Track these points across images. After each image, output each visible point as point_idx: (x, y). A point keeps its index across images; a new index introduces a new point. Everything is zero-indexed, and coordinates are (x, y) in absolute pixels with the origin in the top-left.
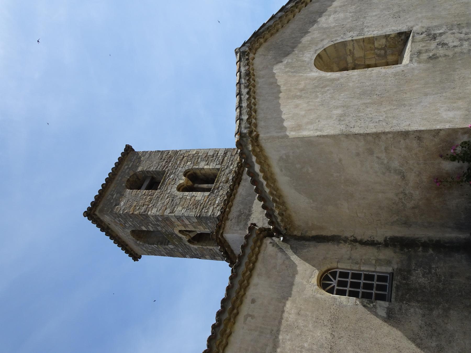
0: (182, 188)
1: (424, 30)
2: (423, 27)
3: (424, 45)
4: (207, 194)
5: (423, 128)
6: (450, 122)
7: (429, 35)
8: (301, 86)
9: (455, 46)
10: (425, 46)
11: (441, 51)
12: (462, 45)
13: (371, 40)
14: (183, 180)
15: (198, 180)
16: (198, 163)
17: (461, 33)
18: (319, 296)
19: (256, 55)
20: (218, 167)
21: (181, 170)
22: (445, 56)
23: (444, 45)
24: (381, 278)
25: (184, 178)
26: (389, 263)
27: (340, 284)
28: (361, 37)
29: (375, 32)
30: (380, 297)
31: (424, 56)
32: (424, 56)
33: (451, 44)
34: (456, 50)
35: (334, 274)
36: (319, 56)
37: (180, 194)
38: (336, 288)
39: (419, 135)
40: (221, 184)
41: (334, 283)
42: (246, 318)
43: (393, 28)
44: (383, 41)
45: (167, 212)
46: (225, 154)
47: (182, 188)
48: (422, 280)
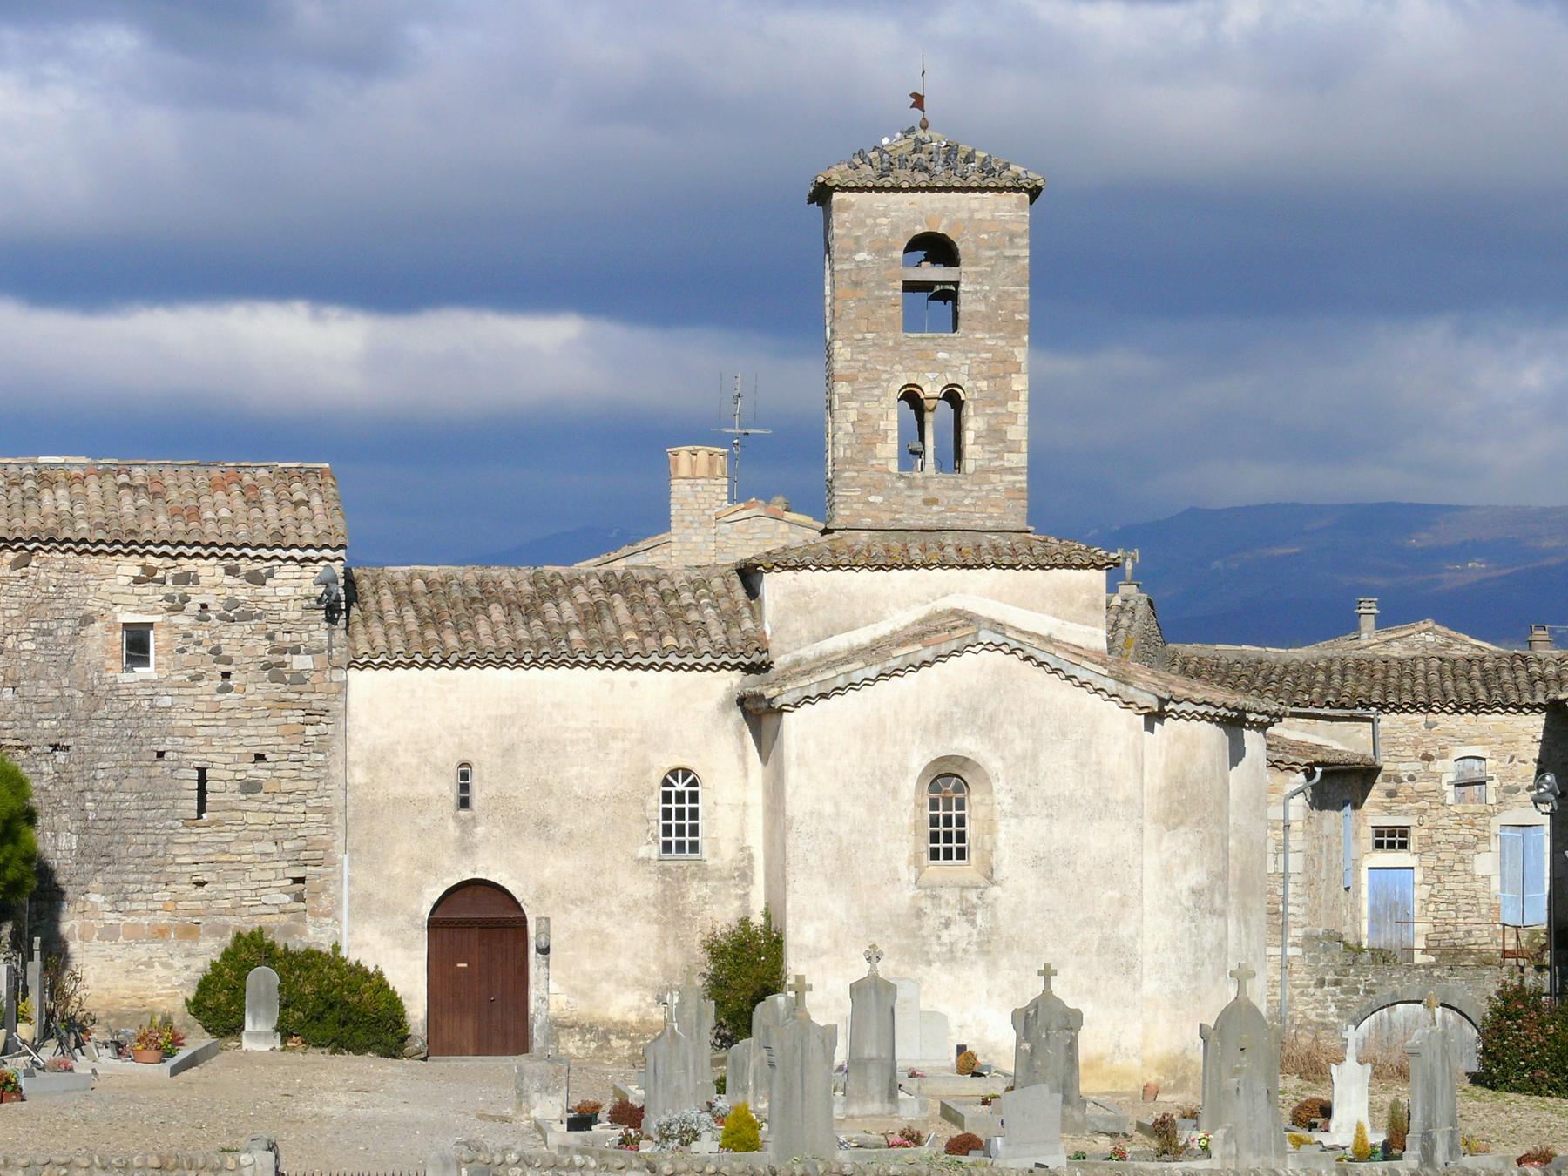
3: (952, 901)
4: (893, 466)
7: (974, 907)
18: (654, 773)
22: (921, 928)
23: (947, 925)
27: (680, 797)
30: (667, 847)
31: (926, 904)
32: (926, 904)
34: (934, 940)
35: (694, 783)
36: (966, 759)
38: (673, 790)
41: (680, 787)
43: (1006, 861)
44: (988, 847)
48: (692, 896)
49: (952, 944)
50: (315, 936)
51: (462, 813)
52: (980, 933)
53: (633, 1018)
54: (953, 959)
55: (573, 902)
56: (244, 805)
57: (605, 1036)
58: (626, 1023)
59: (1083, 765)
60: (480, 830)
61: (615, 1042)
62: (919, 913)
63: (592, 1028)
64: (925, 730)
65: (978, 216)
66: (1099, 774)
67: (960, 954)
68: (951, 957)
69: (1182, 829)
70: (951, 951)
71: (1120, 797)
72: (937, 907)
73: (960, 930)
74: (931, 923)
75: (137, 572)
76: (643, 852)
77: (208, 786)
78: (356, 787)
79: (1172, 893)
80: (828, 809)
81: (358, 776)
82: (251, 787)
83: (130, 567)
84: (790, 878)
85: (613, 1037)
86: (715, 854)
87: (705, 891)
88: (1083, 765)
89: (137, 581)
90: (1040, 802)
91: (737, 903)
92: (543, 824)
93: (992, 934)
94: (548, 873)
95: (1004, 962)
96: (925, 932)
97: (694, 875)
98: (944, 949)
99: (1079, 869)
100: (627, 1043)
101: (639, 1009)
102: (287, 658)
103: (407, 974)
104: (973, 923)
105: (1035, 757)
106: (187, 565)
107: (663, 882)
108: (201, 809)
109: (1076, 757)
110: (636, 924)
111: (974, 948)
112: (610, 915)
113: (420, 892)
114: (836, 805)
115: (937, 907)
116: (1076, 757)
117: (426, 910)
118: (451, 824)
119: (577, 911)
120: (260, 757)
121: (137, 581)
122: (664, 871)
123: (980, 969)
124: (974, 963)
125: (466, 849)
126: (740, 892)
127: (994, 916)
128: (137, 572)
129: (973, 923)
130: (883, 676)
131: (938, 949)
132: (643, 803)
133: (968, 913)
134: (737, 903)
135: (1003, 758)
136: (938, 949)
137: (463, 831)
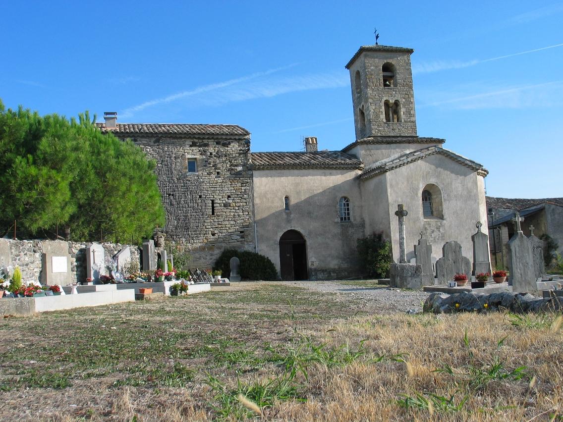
0: (387, 104)
2: (445, 224)
3: (434, 225)
4: (385, 121)
5: (391, 228)
6: (394, 236)
8: (414, 182)
12: (432, 238)
13: (441, 205)
14: (392, 101)
15: (392, 109)
16: (404, 106)
19: (436, 155)
20: (403, 121)
21: (398, 97)
23: (433, 232)
24: (349, 218)
25: (394, 101)
26: (355, 220)
28: (443, 201)
33: (433, 235)
34: (429, 236)
35: (347, 201)
36: (434, 185)
37: (382, 104)
39: (390, 228)
40: (391, 127)
42: (323, 173)
45: (370, 100)
47: (387, 104)
49: (434, 237)
50: (248, 248)
51: (287, 211)
53: (336, 267)
54: (435, 242)
55: (319, 235)
56: (225, 210)
57: (329, 273)
58: (335, 269)
59: (463, 186)
60: (292, 215)
61: (332, 274)
63: (326, 270)
70: (434, 239)
72: (430, 227)
73: (436, 234)
75: (191, 144)
76: (336, 220)
77: (215, 205)
78: (257, 204)
81: (257, 201)
82: (226, 205)
83: (189, 142)
84: (391, 220)
85: (332, 273)
86: (355, 220)
87: (353, 231)
88: (463, 186)
91: (361, 234)
92: (309, 213)
94: (311, 227)
96: (428, 234)
97: (350, 226)
98: (433, 239)
100: (335, 274)
101: (338, 264)
102: (236, 168)
103: (274, 257)
105: (451, 184)
106: (206, 141)
107: (342, 228)
108: (213, 213)
109: (461, 183)
110: (336, 241)
111: (440, 238)
112: (329, 238)
113: (277, 234)
114: (402, 198)
115: (430, 227)
116: (461, 183)
117: (279, 239)
118: (284, 214)
119: (320, 238)
120: (229, 197)
121: (191, 146)
122: (342, 226)
125: (289, 221)
126: (362, 230)
127: (445, 229)
128: (191, 144)
129: (440, 231)
130: (412, 161)
132: (335, 207)
133: (438, 228)
134: (361, 234)
135: (443, 184)
137: (288, 216)
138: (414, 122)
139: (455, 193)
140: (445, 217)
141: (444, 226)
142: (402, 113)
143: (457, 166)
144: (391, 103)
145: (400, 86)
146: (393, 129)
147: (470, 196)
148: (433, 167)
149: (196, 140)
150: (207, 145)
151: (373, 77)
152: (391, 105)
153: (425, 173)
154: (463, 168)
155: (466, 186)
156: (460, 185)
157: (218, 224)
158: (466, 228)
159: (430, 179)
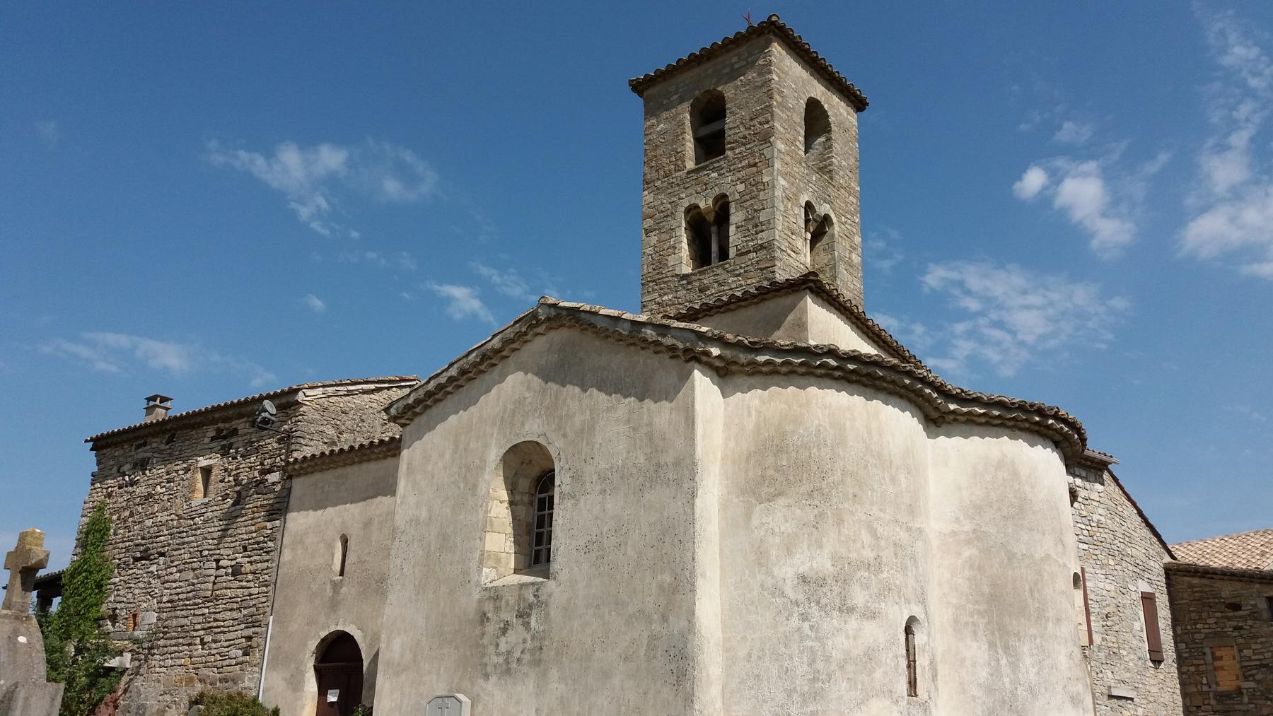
1: (542, 598)
2: (550, 596)
3: (511, 603)
6: (388, 647)
7: (530, 606)
8: (473, 445)
9: (498, 645)
10: (508, 604)
11: (491, 628)
12: (498, 654)
14: (705, 203)
16: (741, 203)
17: (522, 652)
22: (483, 634)
23: (504, 631)
25: (710, 202)
29: (560, 521)
31: (489, 607)
32: (489, 607)
33: (503, 641)
34: (491, 649)
43: (562, 548)
46: (762, 247)
49: (509, 653)
52: (533, 638)
62: (484, 618)
64: (502, 420)
65: (737, 66)
66: (650, 436)
67: (514, 665)
68: (507, 671)
69: (781, 501)
70: (507, 662)
71: (669, 458)
72: (497, 609)
73: (515, 636)
74: (491, 628)
79: (770, 582)
80: (424, 514)
89: (213, 439)
90: (595, 477)
93: (543, 638)
95: (554, 673)
96: (485, 641)
98: (501, 659)
99: (630, 552)
104: (527, 625)
105: (592, 429)
111: (527, 657)
113: (305, 645)
115: (497, 609)
116: (629, 421)
121: (213, 439)
123: (531, 685)
124: (526, 675)
125: (334, 605)
127: (547, 615)
129: (527, 625)
131: (495, 659)
133: (523, 615)
135: (565, 435)
136: (495, 659)
138: (767, 247)
139: (603, 465)
140: (555, 566)
141: (547, 604)
142: (732, 229)
143: (617, 360)
144: (708, 210)
145: (733, 149)
146: (701, 291)
147: (658, 465)
148: (536, 381)
149: (221, 425)
150: (235, 432)
151: (660, 152)
152: (711, 218)
153: (510, 407)
154: (644, 360)
155: (645, 430)
156: (622, 428)
157: (216, 620)
158: (631, 609)
159: (523, 424)
